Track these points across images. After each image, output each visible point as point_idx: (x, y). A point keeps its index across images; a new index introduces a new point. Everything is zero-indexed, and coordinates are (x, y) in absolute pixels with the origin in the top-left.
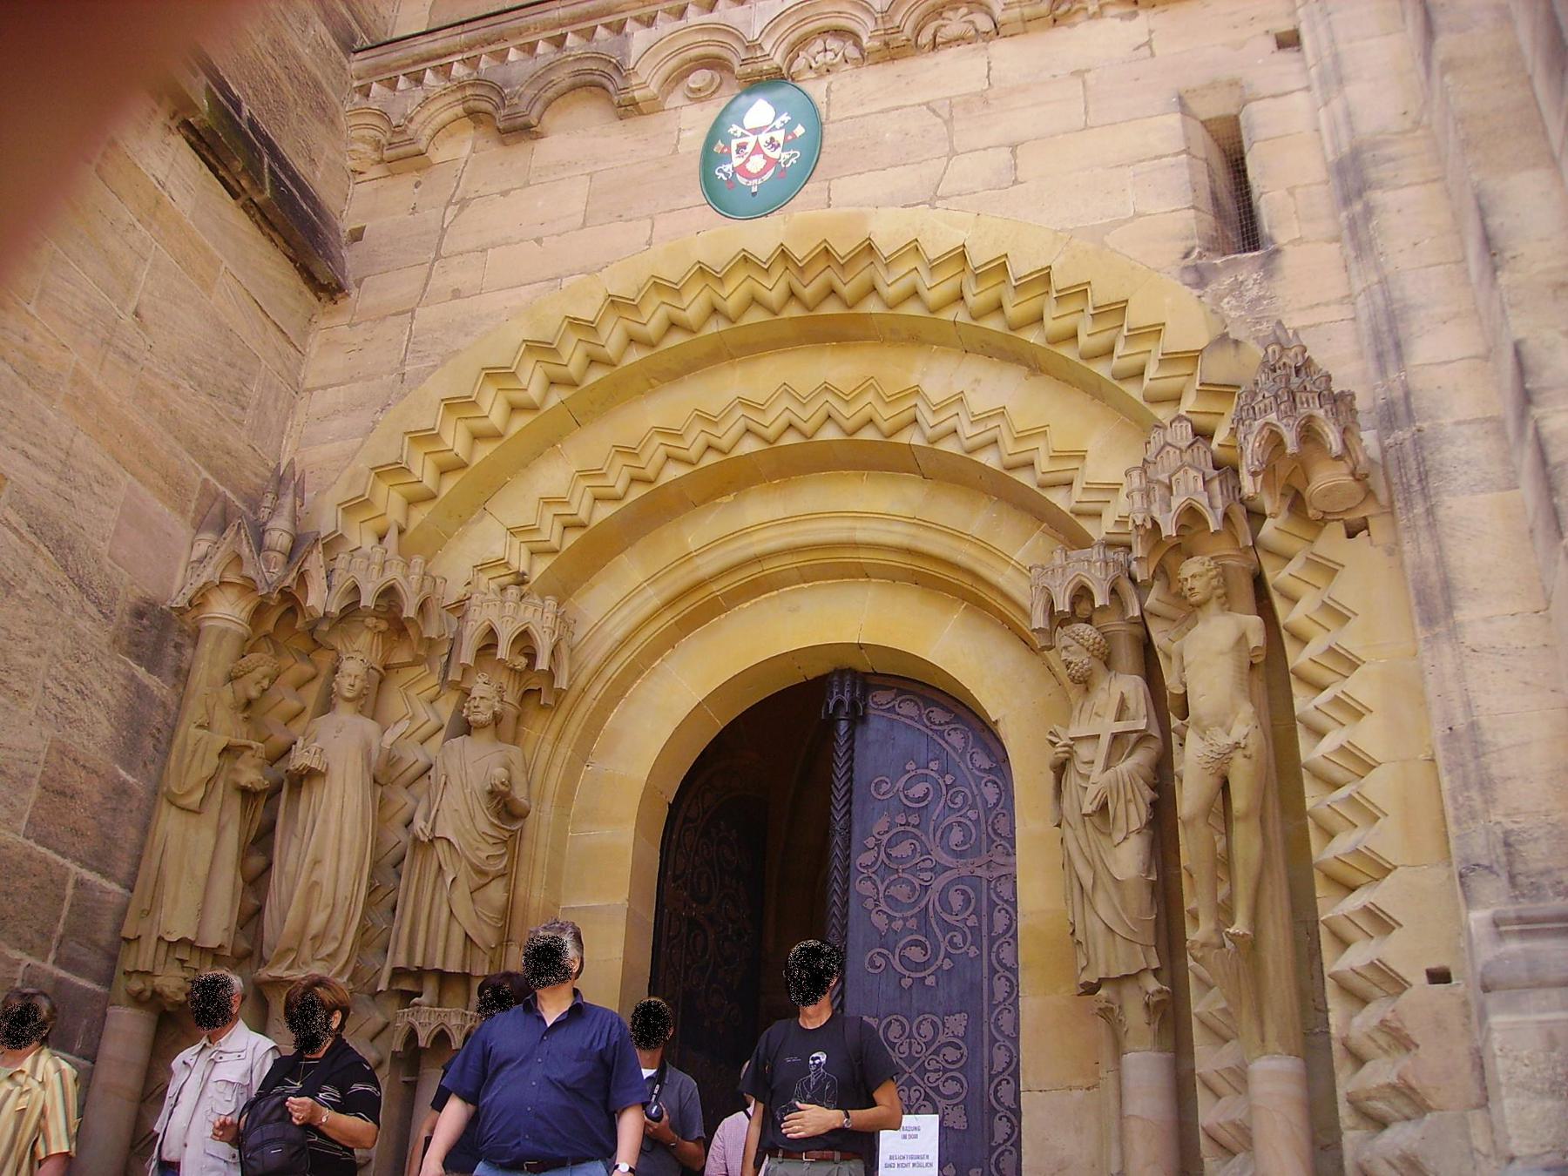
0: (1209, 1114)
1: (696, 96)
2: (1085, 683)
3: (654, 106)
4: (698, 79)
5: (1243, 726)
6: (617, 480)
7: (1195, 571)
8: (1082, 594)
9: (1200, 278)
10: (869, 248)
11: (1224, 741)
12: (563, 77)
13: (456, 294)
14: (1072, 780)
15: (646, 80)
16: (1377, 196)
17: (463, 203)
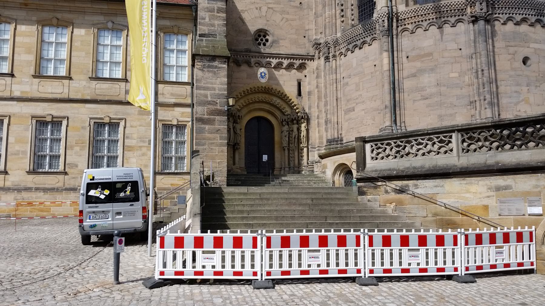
0: (291, 155)
1: (257, 67)
2: (284, 126)
3: (253, 67)
4: (257, 65)
5: (297, 133)
6: (247, 102)
7: (295, 122)
8: (285, 119)
9: (297, 98)
10: (272, 88)
11: (296, 134)
12: (244, 61)
13: (235, 83)
14: (283, 133)
15: (253, 64)
16: (311, 96)
17: (234, 72)
